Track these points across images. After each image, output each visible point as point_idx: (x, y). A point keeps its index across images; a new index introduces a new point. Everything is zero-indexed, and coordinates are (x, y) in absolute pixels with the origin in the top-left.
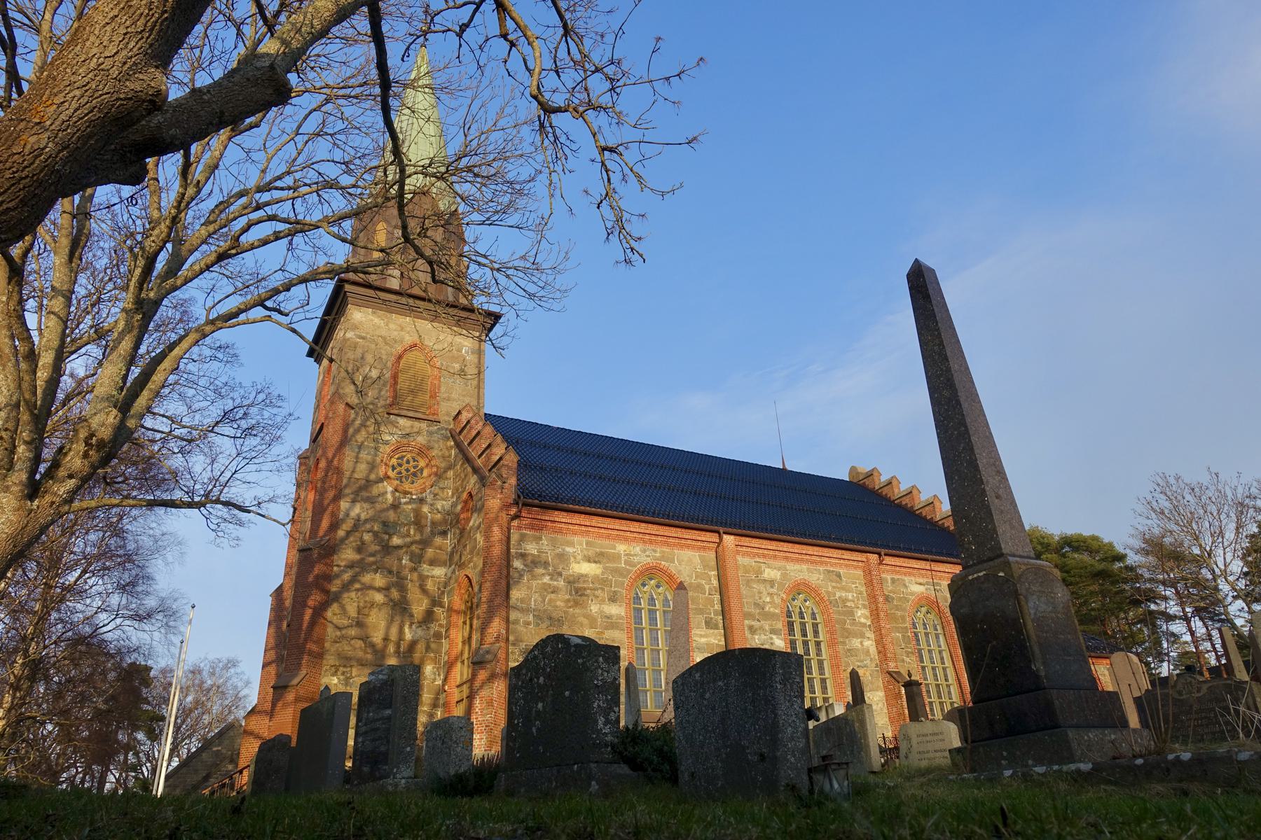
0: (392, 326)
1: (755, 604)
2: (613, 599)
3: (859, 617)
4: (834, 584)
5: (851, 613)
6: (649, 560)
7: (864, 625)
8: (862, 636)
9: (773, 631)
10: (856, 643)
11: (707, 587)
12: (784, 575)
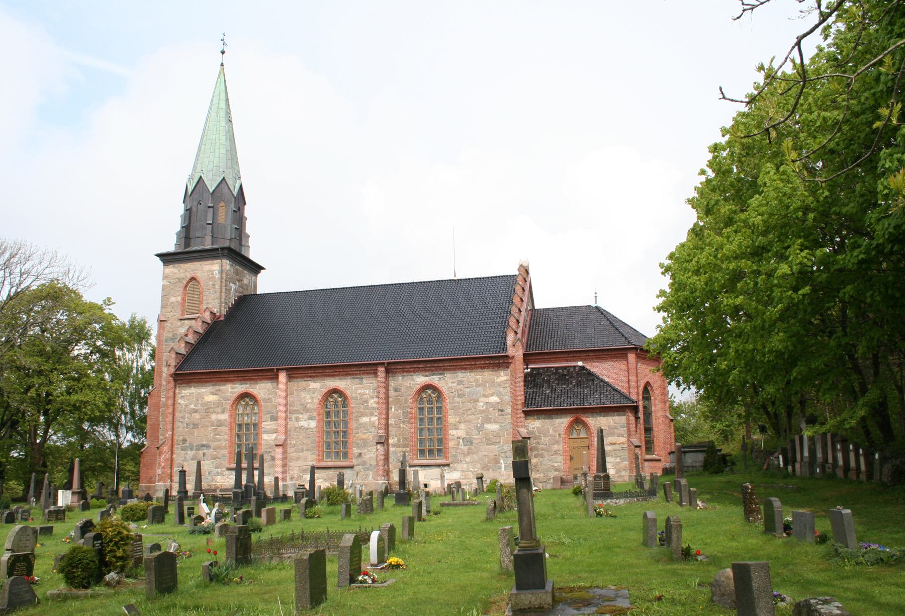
0: (181, 271)
1: (301, 405)
2: (223, 412)
3: (371, 404)
4: (356, 386)
5: (366, 402)
6: (243, 389)
7: (375, 408)
8: (372, 414)
9: (310, 418)
10: (365, 420)
11: (273, 399)
12: (322, 387)
